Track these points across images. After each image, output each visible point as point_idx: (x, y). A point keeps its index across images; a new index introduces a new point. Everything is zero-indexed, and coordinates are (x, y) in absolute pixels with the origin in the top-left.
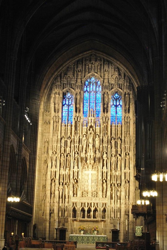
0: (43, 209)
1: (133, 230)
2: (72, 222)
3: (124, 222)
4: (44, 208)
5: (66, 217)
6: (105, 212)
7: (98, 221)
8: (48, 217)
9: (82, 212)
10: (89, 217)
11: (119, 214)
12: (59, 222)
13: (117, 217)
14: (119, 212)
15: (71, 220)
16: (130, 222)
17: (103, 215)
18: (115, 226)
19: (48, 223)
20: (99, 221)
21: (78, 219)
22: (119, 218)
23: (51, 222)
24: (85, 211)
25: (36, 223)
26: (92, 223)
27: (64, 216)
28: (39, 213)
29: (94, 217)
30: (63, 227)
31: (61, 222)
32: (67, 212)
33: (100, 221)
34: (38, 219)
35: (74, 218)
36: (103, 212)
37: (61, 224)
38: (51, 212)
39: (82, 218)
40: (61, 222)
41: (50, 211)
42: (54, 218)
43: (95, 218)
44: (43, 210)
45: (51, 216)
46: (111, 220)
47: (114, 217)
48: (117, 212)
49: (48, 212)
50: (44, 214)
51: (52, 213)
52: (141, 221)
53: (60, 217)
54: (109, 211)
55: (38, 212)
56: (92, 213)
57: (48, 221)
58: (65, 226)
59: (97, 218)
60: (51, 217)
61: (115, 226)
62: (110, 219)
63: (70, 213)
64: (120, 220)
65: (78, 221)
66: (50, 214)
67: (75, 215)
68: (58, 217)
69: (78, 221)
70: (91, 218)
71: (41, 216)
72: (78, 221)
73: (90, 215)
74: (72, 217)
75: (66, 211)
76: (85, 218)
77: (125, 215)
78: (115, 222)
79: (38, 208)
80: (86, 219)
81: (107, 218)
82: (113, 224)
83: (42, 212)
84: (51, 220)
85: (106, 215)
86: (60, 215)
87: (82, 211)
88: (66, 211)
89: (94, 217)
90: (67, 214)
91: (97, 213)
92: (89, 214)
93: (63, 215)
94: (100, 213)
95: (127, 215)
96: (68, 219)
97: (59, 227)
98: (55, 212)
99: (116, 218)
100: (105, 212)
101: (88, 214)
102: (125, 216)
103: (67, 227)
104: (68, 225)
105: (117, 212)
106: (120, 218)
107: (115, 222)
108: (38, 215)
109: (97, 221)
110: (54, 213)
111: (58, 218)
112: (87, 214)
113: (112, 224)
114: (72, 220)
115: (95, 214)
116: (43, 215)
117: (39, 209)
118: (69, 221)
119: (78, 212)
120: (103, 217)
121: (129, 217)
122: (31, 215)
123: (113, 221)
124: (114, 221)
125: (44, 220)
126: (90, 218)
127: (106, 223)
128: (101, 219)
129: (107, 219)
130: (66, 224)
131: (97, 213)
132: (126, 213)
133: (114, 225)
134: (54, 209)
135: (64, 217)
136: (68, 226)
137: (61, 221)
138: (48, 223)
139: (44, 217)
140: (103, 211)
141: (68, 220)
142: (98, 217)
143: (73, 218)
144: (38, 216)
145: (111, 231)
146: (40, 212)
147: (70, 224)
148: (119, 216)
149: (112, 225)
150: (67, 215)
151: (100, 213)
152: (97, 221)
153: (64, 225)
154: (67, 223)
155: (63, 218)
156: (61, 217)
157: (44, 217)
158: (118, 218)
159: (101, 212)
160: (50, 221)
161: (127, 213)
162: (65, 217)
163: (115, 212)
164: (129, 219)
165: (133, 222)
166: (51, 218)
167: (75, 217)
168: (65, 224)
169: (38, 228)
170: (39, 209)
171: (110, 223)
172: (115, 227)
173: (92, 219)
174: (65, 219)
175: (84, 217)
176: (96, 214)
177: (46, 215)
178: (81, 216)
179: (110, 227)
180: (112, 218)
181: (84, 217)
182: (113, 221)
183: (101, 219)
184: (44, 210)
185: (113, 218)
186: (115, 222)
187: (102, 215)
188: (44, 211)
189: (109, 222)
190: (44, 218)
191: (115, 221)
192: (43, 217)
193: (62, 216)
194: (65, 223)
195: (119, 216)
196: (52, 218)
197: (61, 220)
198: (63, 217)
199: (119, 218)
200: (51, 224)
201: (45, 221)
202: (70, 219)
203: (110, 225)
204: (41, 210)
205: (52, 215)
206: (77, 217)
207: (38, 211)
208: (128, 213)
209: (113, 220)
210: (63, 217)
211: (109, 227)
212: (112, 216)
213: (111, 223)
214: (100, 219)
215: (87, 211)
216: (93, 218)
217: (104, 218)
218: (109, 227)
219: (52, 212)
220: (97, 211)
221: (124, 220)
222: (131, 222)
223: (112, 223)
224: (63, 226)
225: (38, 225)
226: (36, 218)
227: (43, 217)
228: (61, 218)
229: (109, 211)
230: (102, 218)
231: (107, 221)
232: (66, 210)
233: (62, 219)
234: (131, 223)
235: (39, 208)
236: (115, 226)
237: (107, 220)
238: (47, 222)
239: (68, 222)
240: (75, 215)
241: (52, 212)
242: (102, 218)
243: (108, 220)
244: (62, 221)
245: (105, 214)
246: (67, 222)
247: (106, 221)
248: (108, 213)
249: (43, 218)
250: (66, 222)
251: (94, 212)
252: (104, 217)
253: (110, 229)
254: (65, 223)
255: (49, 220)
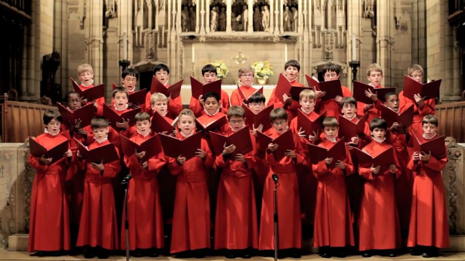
0: (81, 6)
1: (391, 69)
2: (180, 44)
3: (360, 42)
4: (85, 4)
5: (160, 29)
6: (293, 9)
7: (272, 38)
8: (98, 31)
9: (215, 11)
10: (239, 26)
11: (340, 14)
12: (137, 47)
13: (334, 27)
14: (341, 8)
15: (179, 39)
16: (380, 41)
17: (286, 19)
18: (327, 56)
19: (97, 49)
20: (275, 40)
21: (203, 33)
22: (340, 28)
23: (109, 47)
24: (225, 7)
25: (58, 51)
26: (251, 46)
27: (154, 27)
28: (70, 19)
29: (258, 27)
30: (149, 64)
31: (143, 47)
32: (163, 12)
33: (278, 39)
34: (67, 39)
35: (188, 31)
36: (287, 8)
37: (144, 53)
38: (107, 13)
39: (216, 31)
40: (145, 45)
41: (105, 9)
42: (119, 35)
43: (261, 29)
44: (81, 10)
45: (108, 27)
46: (314, 34)
47: (326, 27)
48: (334, 9)
49: (98, 13)
50: (85, 22)
51: (111, 17)
52: (413, 39)
53: (139, 29)
54: (308, 4)
55: (64, 18)
56: (249, 14)
57: (97, 43)
58: (156, 59)
59: (267, 29)
60: (108, 30)
61: (327, 56)
62: (311, 34)
63: (172, 15)
64: (345, 34)
65: (202, 42)
66: (105, 21)
67: (189, 23)
68: (133, 28)
69: (202, 42)
70: (247, 30)
71: (78, 30)
72: (201, 39)
73: (241, 22)
74: (179, 29)
75: (159, 10)
76: (224, 30)
77: (363, 17)
78: (329, 42)
79: (64, 5)
80: (229, 32)
81: (300, 29)
82: (321, 49)
83: (79, 18)
84: (110, 40)
85: (297, 18)
86: (140, 22)
87: (216, 6)
88: (159, 10)
89: (258, 27)
90: (164, 19)
91: (265, 13)
92: (238, 18)
93: (150, 21)
94: (277, 12)
95: (369, 17)
96: (166, 34)
97: (139, 64)
98: (122, 15)
99: (330, 30)
100: (293, 9)
101: (237, 16)
102: (364, 20)
103: (166, 62)
104: (166, 55)
105: (334, 9)
106: (346, 28)
107: (327, 44)
108: (64, 27)
109: (267, 41)
110: (117, 16)
111: (134, 34)
112: (232, 17)
113: (317, 49)
114: (181, 37)
115: (261, 16)
116: (82, 27)
117: (70, 6)
118: (170, 42)
119: (203, 12)
120: (289, 26)
121: (376, 24)
122: (28, 16)
123: (321, 37)
124: (324, 39)
125: (87, 41)
126: (242, 30)
127: (298, 46)
128: (280, 32)
129: (301, 32)
130: (160, 53)
131: (267, 11)
132: (367, 12)
133: (324, 51)
134: (118, 4)
135: (154, 30)
136: (166, 58)
137: (145, 42)
138: (97, 49)
139: (86, 32)
140: (288, 5)
141: (168, 38)
142: (269, 26)
143: (183, 31)
144: (67, 29)
145: (315, 71)
146: (75, 18)
147: (176, 50)
148: (340, 22)
149: (319, 53)
150: (163, 23)
151: (277, 12)
152: (267, 41)
153: (152, 55)
154: (164, 49)
155: (152, 33)
156: (142, 30)
157: (86, 32)
158: (338, 28)
159: (279, 10)
160: (105, 45)
161: (369, 10)
162: (157, 29)
163: (326, 10)
164: (375, 30)
165: (388, 39)
166: (108, 34)
167: (193, 30)
168: (156, 51)
169: (67, 70)
170: (70, 6)
171: (311, 45)
172: (328, 59)
173: (250, 32)
174: (156, 36)
175: (221, 27)
176: (264, 19)
177: (91, 26)
178: (210, 24)
179: (310, 60)
180: (319, 28)
181: (221, 27)
182: (321, 37)
183: (280, 32)
184: (85, 9)
185: (323, 29)
186: (329, 42)
187: (284, 21)
188: (85, 13)
189: (309, 42)
190: (87, 36)
191: (329, 38)
192: (82, 32)
193: (146, 26)
194: (156, 48)
195: (340, 22)
196: (114, 34)
197: (143, 43)
198: (149, 29)
199: (340, 28)
200: (109, 54)
201: (88, 44)
202: (173, 34)
203: (311, 52)
204: (76, 10)
205: (111, 23)
206: (197, 29)
207: (64, 15)
208: (372, 13)
209: (323, 34)
210: (149, 29)
211: (309, 58)
212: (316, 23)
213: (315, 47)
214: (277, 34)
215: (233, 7)
216: (255, 30)
217: (292, 29)
218: (309, 58)
219: (113, 12)
220: (266, 7)
221: (361, 34)
222: (385, 40)
223: (319, 47)
224: (150, 61)
225: (67, 58)
226: (57, 35)
227: (82, 32)
228: (143, 36)
229: (308, 4)
230: (286, 29)
231: (303, 39)
232: (159, 5)
233: (146, 34)
234: (383, 44)
235: (67, 3)
236: (328, 54)
237: (303, 36)
238: (94, 47)
239: (168, 45)
240: (189, 23)
241: (113, 12)
242: (286, 29)
243: (306, 34)
244: (148, 42)
245: (296, 15)
246: (165, 46)
247: (300, 39)
248: (305, 12)
249: (84, 36)
250: (160, 46)
251: (257, 9)
252: (290, 25)
253: (312, 65)
254: (158, 49)
255: (102, 41)
